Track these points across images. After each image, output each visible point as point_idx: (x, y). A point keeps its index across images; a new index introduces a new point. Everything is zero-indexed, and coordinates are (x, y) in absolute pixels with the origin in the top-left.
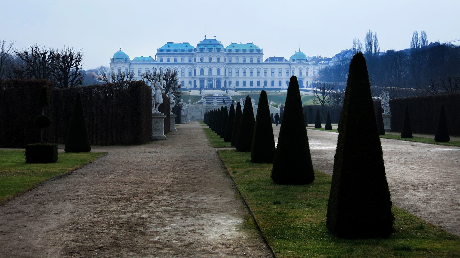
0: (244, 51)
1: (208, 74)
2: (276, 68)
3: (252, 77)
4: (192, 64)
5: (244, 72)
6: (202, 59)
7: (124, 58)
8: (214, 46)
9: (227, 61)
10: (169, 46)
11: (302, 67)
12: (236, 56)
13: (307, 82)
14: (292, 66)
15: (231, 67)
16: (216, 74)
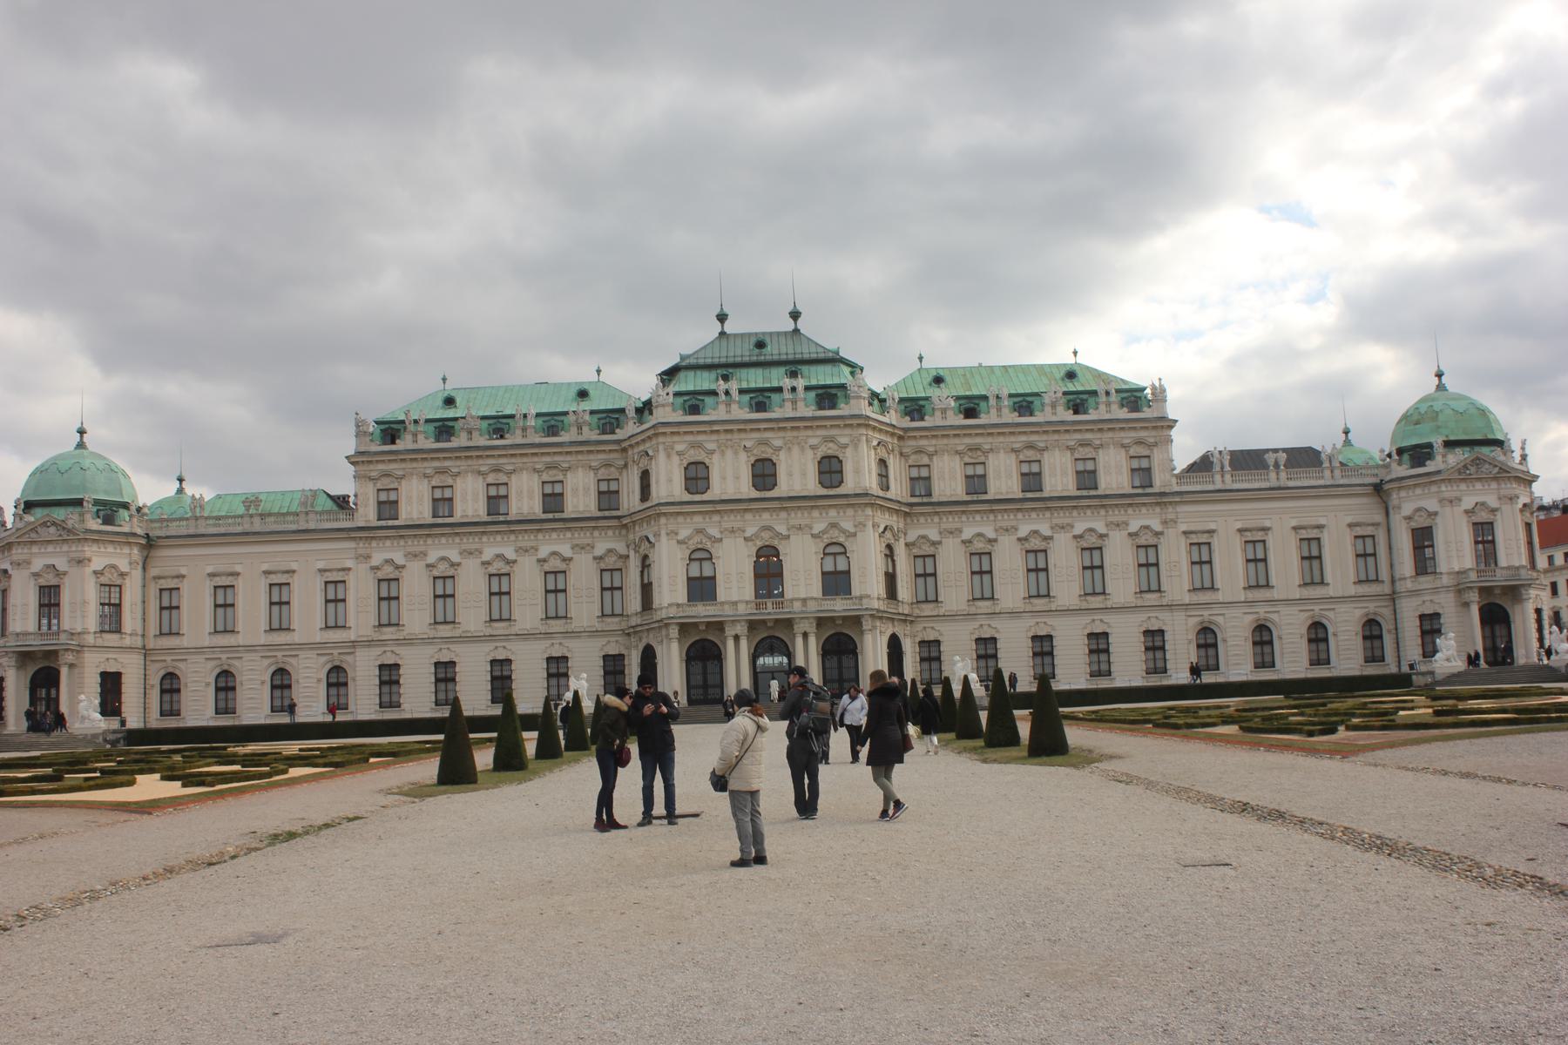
0: (1024, 404)
1: (748, 592)
2: (1282, 524)
3: (1096, 602)
4: (624, 524)
5: (1038, 571)
6: (696, 477)
7: (89, 496)
8: (794, 375)
9: (899, 489)
11: (1492, 501)
12: (962, 443)
13: (1538, 611)
14: (1407, 504)
15: (934, 536)
16: (816, 589)
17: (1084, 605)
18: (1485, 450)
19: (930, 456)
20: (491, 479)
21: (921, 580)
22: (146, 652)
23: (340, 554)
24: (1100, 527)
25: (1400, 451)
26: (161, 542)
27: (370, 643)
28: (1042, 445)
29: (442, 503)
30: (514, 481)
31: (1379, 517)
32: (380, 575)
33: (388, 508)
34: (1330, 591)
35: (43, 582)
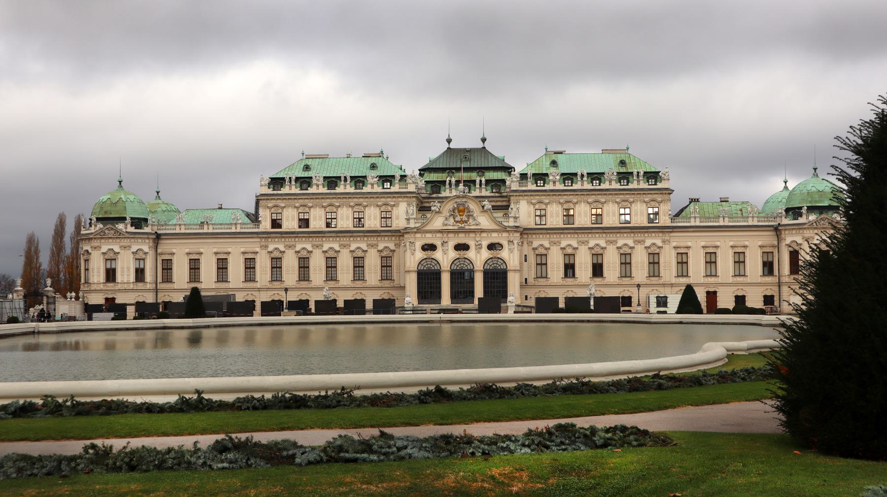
10: (307, 168)
14: (789, 238)
15: (547, 244)
17: (620, 282)
18: (830, 213)
19: (547, 204)
20: (328, 210)
21: (539, 267)
22: (156, 291)
23: (252, 245)
24: (632, 245)
25: (787, 210)
26: (163, 237)
27: (268, 289)
28: (603, 200)
29: (304, 223)
30: (340, 211)
31: (776, 243)
32: (273, 255)
33: (276, 224)
34: (748, 280)
35: (106, 257)
